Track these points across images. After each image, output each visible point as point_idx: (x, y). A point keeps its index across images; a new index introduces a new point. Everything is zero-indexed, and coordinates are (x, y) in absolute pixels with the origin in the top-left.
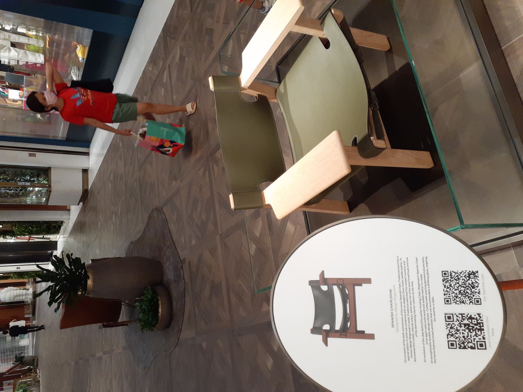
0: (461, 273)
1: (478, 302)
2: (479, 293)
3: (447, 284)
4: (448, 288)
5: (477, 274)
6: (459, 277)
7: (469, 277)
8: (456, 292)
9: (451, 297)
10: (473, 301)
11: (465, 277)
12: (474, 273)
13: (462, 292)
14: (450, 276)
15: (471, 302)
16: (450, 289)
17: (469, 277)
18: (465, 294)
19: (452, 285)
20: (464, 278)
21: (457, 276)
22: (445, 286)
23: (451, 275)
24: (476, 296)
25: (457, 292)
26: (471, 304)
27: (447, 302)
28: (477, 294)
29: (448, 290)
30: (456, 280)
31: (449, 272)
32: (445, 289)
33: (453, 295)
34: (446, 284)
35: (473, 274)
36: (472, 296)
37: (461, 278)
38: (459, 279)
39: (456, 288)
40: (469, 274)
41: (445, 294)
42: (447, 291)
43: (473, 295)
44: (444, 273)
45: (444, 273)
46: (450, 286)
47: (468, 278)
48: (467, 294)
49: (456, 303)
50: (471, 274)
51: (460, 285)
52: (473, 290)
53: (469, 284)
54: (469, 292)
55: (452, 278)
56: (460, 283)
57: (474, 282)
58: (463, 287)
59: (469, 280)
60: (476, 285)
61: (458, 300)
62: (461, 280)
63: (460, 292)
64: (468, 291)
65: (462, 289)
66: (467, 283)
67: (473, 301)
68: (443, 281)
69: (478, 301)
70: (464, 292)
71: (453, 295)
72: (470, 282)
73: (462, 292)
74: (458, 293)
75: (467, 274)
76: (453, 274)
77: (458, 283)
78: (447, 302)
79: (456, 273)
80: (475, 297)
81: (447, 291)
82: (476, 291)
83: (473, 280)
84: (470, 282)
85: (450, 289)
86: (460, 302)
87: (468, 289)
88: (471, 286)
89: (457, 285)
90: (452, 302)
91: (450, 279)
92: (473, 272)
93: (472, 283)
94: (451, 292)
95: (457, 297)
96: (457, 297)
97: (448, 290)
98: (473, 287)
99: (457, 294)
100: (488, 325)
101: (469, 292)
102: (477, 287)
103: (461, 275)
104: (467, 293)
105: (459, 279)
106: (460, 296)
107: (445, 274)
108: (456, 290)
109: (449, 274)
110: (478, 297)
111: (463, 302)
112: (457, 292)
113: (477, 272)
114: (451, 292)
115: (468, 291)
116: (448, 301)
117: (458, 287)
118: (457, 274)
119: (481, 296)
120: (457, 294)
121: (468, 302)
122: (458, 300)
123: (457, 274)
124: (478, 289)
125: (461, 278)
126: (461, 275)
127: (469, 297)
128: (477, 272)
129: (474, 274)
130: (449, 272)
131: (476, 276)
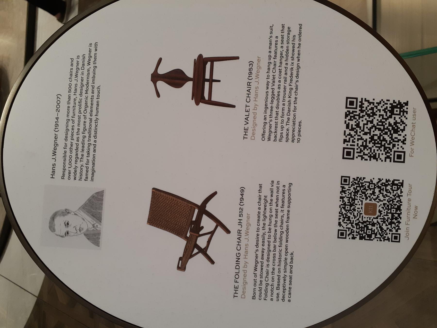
0: (379, 104)
1: (400, 158)
2: (404, 142)
3: (353, 123)
4: (352, 129)
5: (405, 108)
6: (375, 110)
7: (392, 112)
8: (365, 137)
9: (356, 147)
10: (392, 157)
11: (384, 110)
12: (400, 105)
13: (376, 138)
14: (359, 108)
15: (388, 157)
16: (356, 132)
17: (392, 112)
18: (379, 142)
19: (361, 125)
20: (382, 113)
21: (372, 109)
22: (347, 127)
23: (361, 106)
24: (399, 146)
25: (367, 137)
26: (388, 160)
27: (347, 155)
28: (400, 144)
29: (353, 133)
30: (369, 116)
31: (359, 100)
32: (348, 132)
33: (360, 142)
34: (351, 123)
35: (400, 107)
36: (391, 146)
37: (378, 113)
38: (374, 114)
39: (366, 130)
40: (393, 107)
41: (345, 141)
42: (350, 134)
43: (394, 146)
44: (350, 102)
45: (350, 102)
46: (358, 125)
47: (389, 114)
48: (383, 143)
49: (362, 158)
50: (396, 107)
51: (374, 126)
52: (395, 135)
53: (390, 124)
54: (388, 139)
55: (362, 111)
56: (375, 122)
57: (399, 121)
58: (380, 129)
59: (390, 117)
60: (402, 128)
61: (366, 152)
62: (377, 117)
63: (372, 138)
64: (386, 137)
65: (377, 132)
66: (387, 122)
67: (392, 157)
68: (346, 116)
69: (399, 157)
70: (379, 138)
71: (360, 142)
72: (392, 121)
73: (376, 138)
74: (369, 140)
75: (389, 106)
76: (366, 104)
77: (372, 122)
78: (347, 155)
79: (370, 103)
80: (395, 149)
81: (350, 134)
82: (399, 137)
83: (397, 117)
84: (392, 121)
85: (356, 132)
86: (370, 157)
87: (386, 133)
88: (393, 128)
89: (370, 125)
90: (356, 155)
91: (358, 112)
92: (400, 103)
93: (396, 123)
94: (356, 137)
95: (365, 147)
96: (365, 147)
97: (353, 133)
98: (396, 132)
99: (366, 141)
100: (409, 200)
101: (388, 139)
102: (403, 130)
103: (379, 107)
104: (384, 140)
105: (374, 114)
106: (370, 145)
107: (352, 103)
108: (366, 134)
109: (359, 104)
110: (400, 149)
111: (375, 157)
112: (367, 137)
113: (407, 104)
114: (356, 137)
115: (386, 137)
116: (349, 154)
117: (370, 129)
118: (372, 106)
119: (407, 148)
120: (366, 141)
121: (383, 157)
122: (366, 152)
123: (372, 106)
124: (403, 134)
125: (378, 113)
126: (379, 107)
127: (385, 148)
128: (407, 104)
129: (402, 106)
130: (359, 100)
131: (404, 111)
